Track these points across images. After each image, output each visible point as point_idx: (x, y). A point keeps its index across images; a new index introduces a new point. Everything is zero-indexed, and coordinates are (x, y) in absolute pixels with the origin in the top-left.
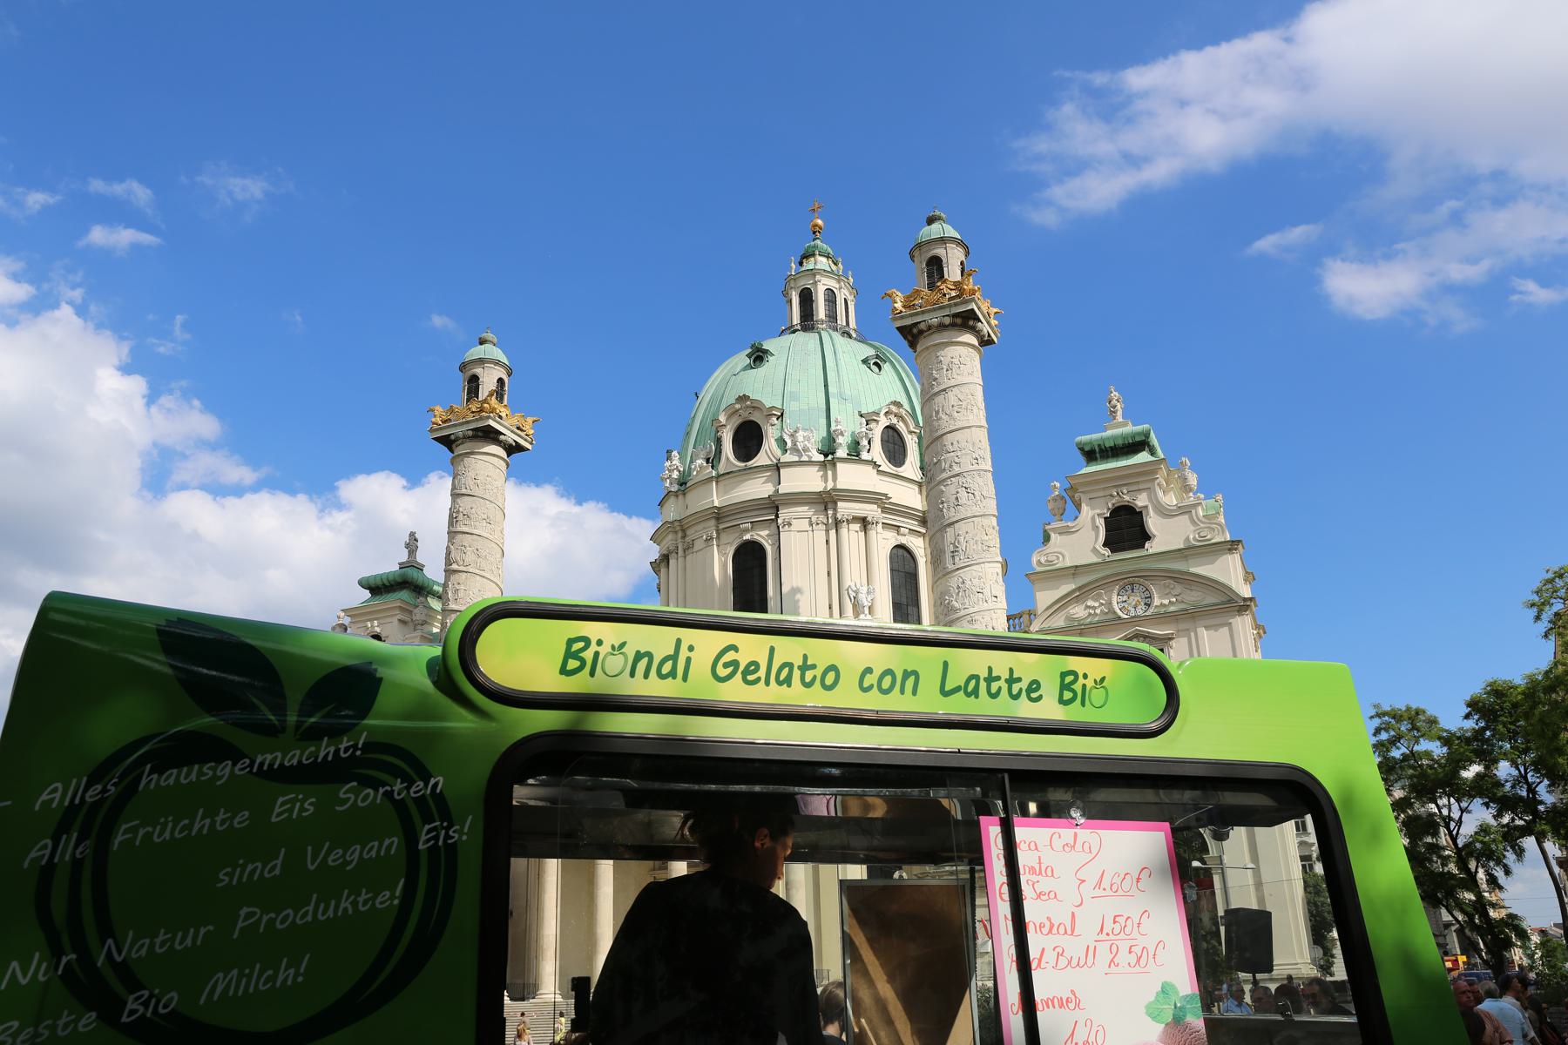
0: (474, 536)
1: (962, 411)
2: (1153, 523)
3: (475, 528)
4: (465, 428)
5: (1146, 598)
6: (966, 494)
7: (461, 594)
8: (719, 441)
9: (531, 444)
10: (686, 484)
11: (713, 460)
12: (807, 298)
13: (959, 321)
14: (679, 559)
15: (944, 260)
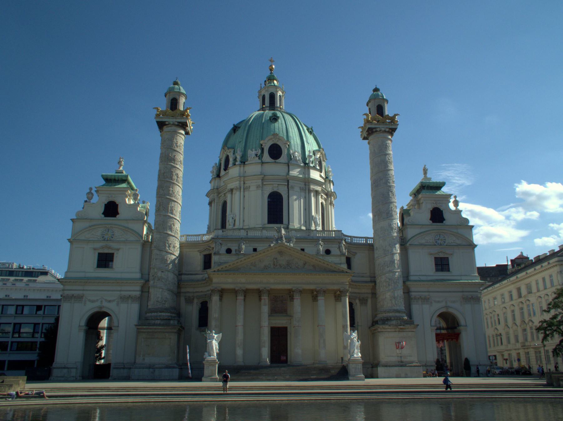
0: (176, 169)
1: (390, 163)
2: (446, 216)
3: (177, 164)
4: (174, 120)
5: (444, 240)
6: (391, 194)
7: (171, 192)
8: (262, 150)
9: (191, 132)
10: (244, 163)
11: (259, 156)
12: (272, 97)
13: (390, 131)
14: (242, 193)
15: (383, 106)
